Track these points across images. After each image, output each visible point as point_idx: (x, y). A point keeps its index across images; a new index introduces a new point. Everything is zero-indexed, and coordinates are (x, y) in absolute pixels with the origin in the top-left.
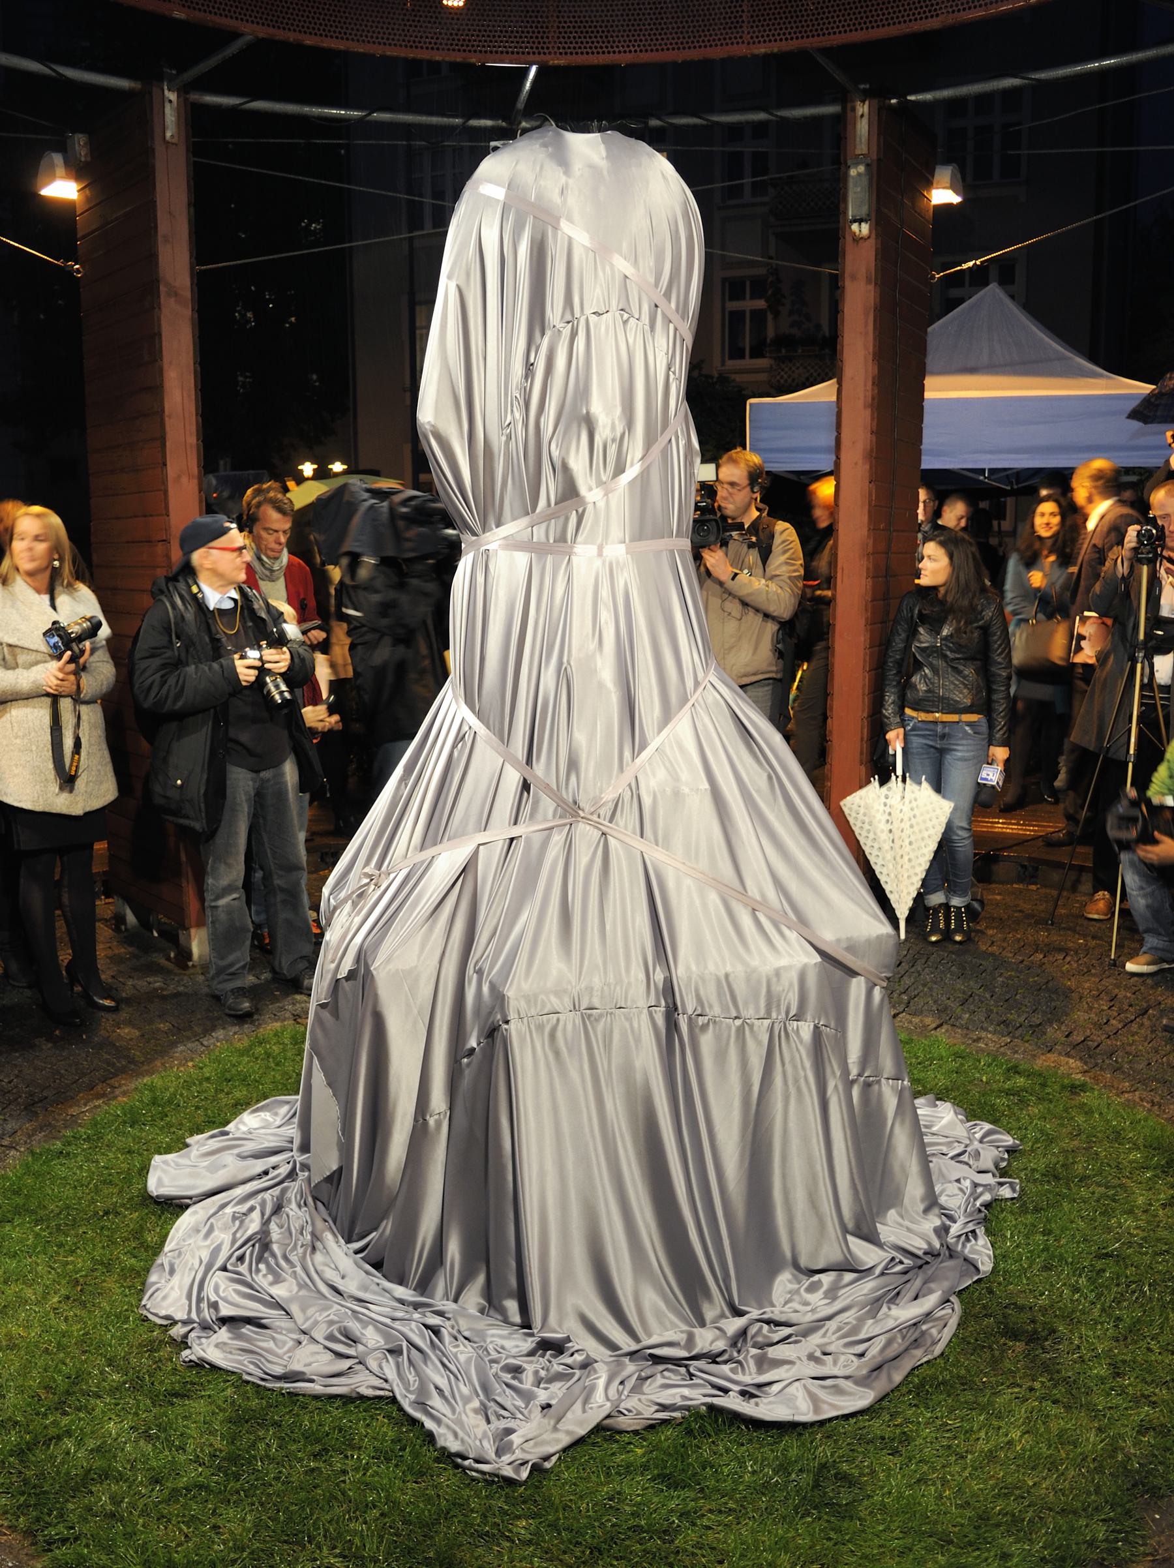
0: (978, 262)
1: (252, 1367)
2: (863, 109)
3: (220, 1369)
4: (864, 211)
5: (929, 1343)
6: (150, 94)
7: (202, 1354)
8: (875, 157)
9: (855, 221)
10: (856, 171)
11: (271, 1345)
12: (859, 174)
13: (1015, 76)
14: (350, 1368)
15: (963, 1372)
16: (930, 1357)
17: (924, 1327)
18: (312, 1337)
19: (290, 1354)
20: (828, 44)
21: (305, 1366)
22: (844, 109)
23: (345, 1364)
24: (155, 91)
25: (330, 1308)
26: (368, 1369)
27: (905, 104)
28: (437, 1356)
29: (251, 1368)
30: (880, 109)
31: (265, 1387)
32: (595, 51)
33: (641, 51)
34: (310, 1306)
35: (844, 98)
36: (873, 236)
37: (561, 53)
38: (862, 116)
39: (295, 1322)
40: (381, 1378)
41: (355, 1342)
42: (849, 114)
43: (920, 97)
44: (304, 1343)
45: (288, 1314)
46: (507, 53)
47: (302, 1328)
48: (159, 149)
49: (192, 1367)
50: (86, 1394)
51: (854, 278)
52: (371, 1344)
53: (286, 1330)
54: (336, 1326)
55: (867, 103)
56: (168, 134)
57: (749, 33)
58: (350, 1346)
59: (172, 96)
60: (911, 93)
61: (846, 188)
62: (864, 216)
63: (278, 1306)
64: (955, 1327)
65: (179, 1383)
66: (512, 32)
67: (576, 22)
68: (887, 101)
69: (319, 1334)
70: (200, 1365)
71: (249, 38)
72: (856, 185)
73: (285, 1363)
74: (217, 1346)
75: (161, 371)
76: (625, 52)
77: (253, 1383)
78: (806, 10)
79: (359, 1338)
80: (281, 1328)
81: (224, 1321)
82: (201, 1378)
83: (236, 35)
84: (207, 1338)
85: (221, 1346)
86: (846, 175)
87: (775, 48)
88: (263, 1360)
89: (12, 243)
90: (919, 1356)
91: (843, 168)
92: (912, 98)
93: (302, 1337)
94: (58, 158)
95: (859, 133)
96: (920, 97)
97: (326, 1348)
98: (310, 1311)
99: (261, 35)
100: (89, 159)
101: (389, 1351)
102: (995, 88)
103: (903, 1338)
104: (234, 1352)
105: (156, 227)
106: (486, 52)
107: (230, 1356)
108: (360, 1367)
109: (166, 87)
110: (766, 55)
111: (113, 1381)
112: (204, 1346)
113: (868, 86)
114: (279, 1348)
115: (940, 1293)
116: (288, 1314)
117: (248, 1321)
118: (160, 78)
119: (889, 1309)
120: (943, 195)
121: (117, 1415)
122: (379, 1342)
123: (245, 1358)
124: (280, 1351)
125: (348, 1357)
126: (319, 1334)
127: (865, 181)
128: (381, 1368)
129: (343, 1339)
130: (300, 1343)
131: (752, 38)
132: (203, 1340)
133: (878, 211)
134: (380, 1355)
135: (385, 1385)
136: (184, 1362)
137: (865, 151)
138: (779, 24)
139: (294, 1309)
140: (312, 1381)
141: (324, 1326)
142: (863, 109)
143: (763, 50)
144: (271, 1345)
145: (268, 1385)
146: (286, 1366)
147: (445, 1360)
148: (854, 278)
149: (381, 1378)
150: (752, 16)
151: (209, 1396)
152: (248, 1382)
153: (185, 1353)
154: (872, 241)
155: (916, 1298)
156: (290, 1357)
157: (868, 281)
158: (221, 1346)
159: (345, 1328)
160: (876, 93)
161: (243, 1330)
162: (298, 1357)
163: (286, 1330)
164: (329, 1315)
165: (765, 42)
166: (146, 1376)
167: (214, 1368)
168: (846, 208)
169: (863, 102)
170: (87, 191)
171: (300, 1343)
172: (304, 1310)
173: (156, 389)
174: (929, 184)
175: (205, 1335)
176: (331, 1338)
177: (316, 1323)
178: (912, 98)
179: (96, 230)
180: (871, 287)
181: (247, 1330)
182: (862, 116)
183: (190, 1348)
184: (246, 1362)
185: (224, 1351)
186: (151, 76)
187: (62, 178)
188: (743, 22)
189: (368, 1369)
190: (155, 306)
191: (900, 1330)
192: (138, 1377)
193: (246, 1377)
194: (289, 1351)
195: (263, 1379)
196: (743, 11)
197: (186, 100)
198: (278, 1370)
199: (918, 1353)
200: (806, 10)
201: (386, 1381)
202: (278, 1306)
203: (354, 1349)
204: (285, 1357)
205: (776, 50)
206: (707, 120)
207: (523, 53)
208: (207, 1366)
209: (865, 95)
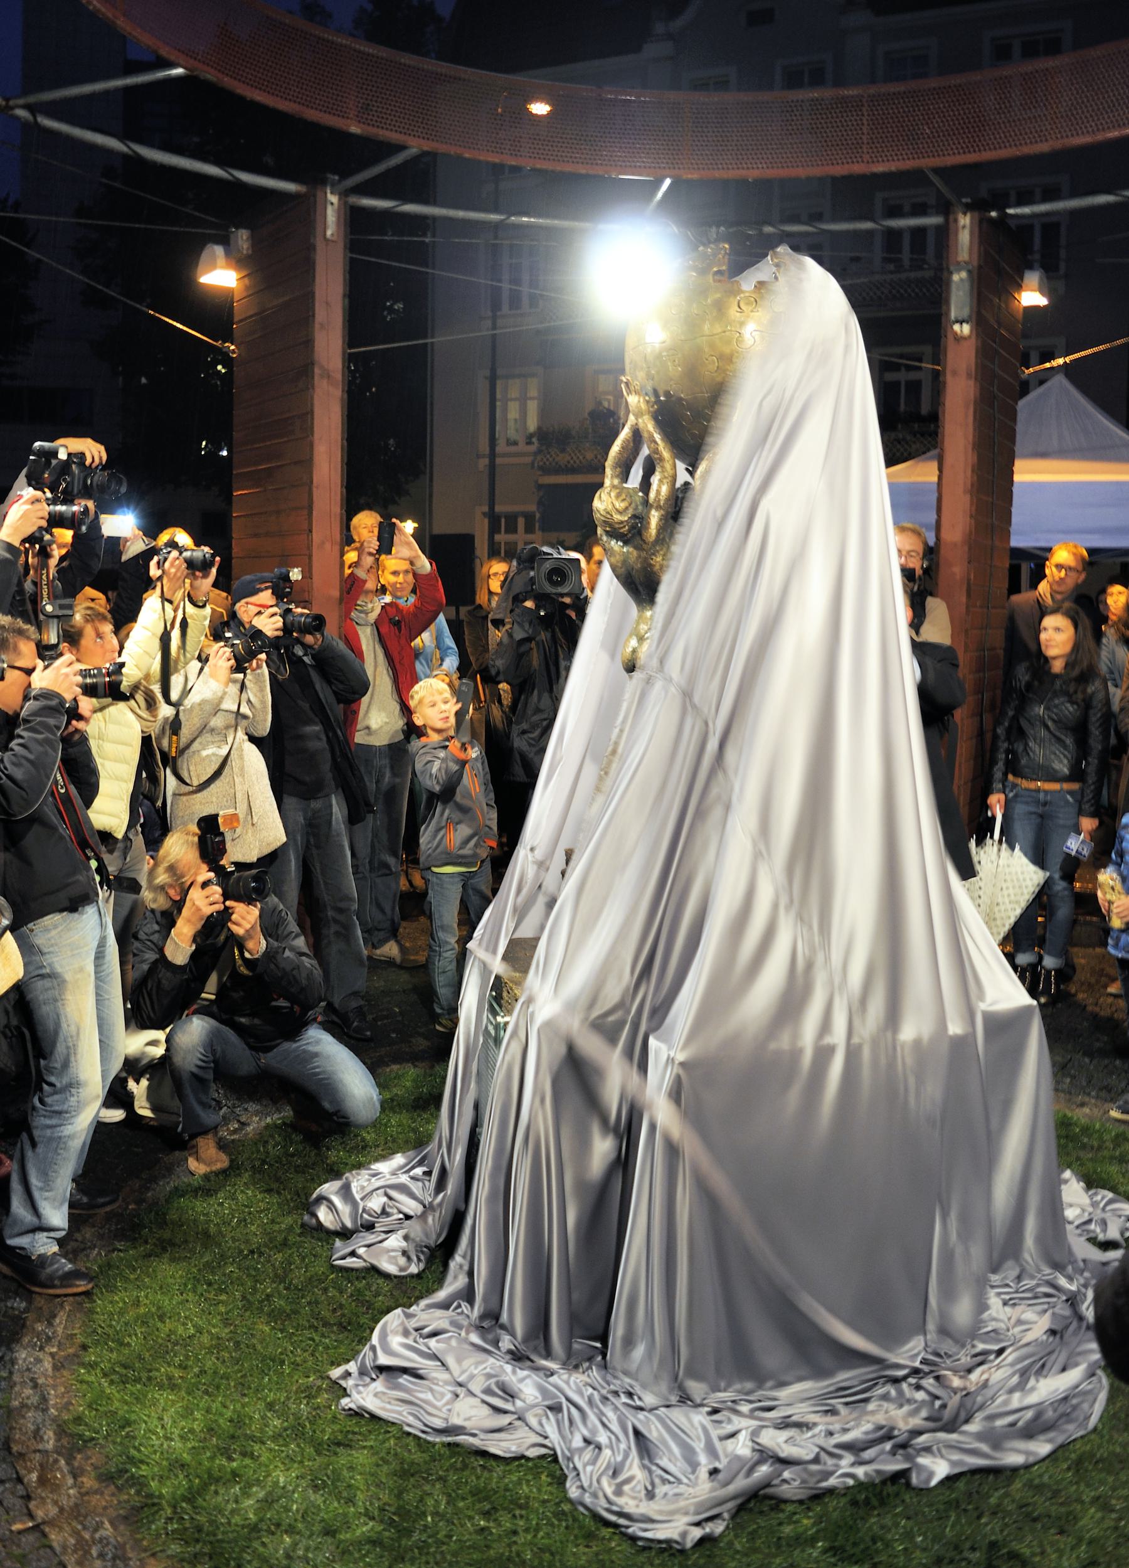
2: (965, 220)
4: (966, 312)
5: (1082, 1418)
6: (315, 196)
7: (362, 1403)
8: (975, 263)
9: (957, 321)
10: (959, 277)
11: (428, 1396)
12: (961, 280)
13: (1109, 192)
15: (1118, 1450)
17: (1074, 1401)
19: (449, 1407)
21: (466, 1420)
23: (504, 1420)
24: (319, 194)
25: (486, 1361)
26: (527, 1425)
27: (1004, 216)
28: (595, 1414)
29: (411, 1420)
30: (981, 222)
31: (426, 1441)
34: (466, 1358)
35: (946, 209)
36: (974, 337)
38: (964, 227)
39: (451, 1373)
40: (541, 1435)
41: (512, 1397)
42: (952, 225)
44: (461, 1396)
45: (443, 1365)
47: (460, 1380)
48: (320, 245)
49: (351, 1415)
50: (252, 1438)
51: (955, 373)
52: (530, 1400)
54: (493, 1380)
56: (329, 233)
58: (507, 1400)
59: (334, 199)
60: (1010, 207)
63: (435, 1357)
65: (341, 1432)
69: (476, 1387)
70: (357, 1414)
71: (414, 151)
73: (445, 1416)
74: (376, 1395)
77: (415, 1436)
81: (382, 1369)
82: (361, 1427)
83: (402, 148)
84: (364, 1386)
86: (948, 282)
89: (175, 323)
90: (1073, 1431)
91: (945, 274)
92: (1011, 211)
93: (459, 1390)
94: (219, 250)
97: (484, 1402)
98: (466, 1363)
99: (425, 148)
100: (250, 252)
101: (550, 1408)
104: (393, 1402)
105: (314, 316)
107: (388, 1406)
108: (518, 1423)
109: (329, 191)
111: (275, 1427)
113: (969, 200)
114: (439, 1401)
116: (443, 1365)
117: (405, 1371)
118: (324, 182)
120: (1032, 297)
123: (404, 1409)
124: (439, 1404)
125: (505, 1412)
126: (476, 1387)
127: (967, 286)
128: (541, 1424)
129: (500, 1393)
130: (457, 1396)
132: (361, 1388)
135: (546, 1442)
136: (344, 1410)
139: (450, 1361)
140: (474, 1435)
141: (482, 1379)
142: (965, 220)
145: (429, 1438)
146: (446, 1420)
147: (604, 1419)
151: (372, 1447)
152: (409, 1434)
153: (345, 1402)
155: (1064, 1370)
156: (450, 1410)
157: (969, 376)
159: (503, 1383)
160: (978, 206)
161: (401, 1380)
167: (374, 1417)
168: (949, 310)
169: (965, 214)
170: (246, 281)
172: (459, 1361)
174: (1019, 287)
175: (361, 1383)
176: (488, 1391)
178: (1011, 211)
179: (251, 316)
180: (971, 383)
181: (404, 1380)
182: (964, 227)
183: (349, 1396)
184: (405, 1413)
185: (383, 1401)
186: (315, 178)
187: (222, 267)
189: (527, 1425)
193: (407, 1429)
194: (447, 1403)
195: (423, 1432)
197: (346, 203)
198: (439, 1423)
199: (1071, 1427)
201: (546, 1438)
202: (435, 1357)
205: (893, 169)
208: (367, 1415)
209: (968, 208)
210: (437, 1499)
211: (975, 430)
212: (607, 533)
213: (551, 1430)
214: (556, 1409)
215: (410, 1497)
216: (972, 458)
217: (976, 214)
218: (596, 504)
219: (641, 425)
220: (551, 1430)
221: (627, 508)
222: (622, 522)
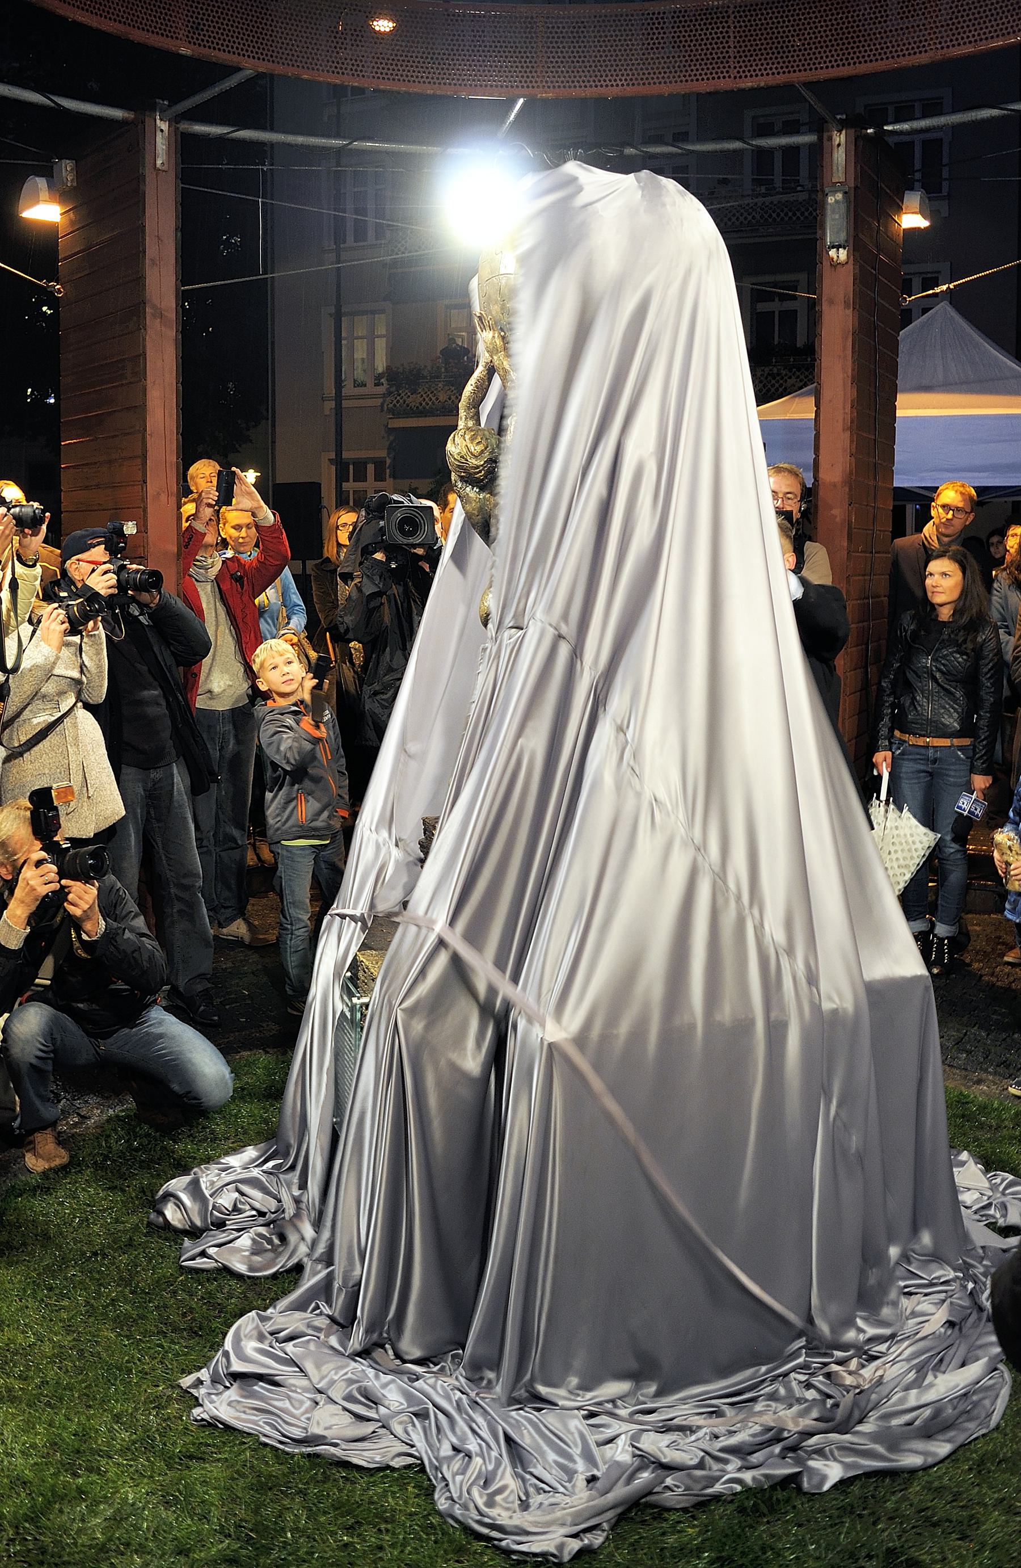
0: (951, 286)
1: (268, 1428)
2: (840, 138)
3: (235, 1429)
4: (843, 236)
9: (833, 247)
11: (286, 1404)
12: (837, 201)
14: (374, 1432)
16: (984, 1431)
18: (329, 1397)
20: (814, 79)
21: (326, 1429)
22: (820, 139)
23: (368, 1428)
25: (347, 1366)
26: (392, 1434)
27: (881, 134)
29: (267, 1430)
31: (283, 1451)
32: (583, 85)
33: (628, 85)
35: (820, 127)
36: (851, 262)
37: (549, 87)
38: (839, 145)
39: (309, 1379)
40: (407, 1444)
41: (376, 1404)
42: (826, 143)
43: (897, 127)
44: (321, 1403)
45: (302, 1371)
46: (496, 86)
50: (98, 1452)
51: (831, 302)
52: (394, 1406)
53: (300, 1388)
55: (844, 132)
57: (735, 67)
58: (371, 1408)
60: (888, 124)
61: (823, 215)
62: (842, 243)
64: (1007, 1399)
65: (194, 1444)
66: (501, 67)
67: (564, 57)
68: (864, 131)
69: (337, 1394)
70: (211, 1425)
72: (833, 212)
74: (229, 1404)
75: (145, 390)
76: (612, 85)
77: (272, 1446)
78: (793, 46)
79: (380, 1399)
80: (294, 1386)
81: (236, 1376)
85: (234, 1404)
86: (824, 203)
87: (762, 82)
88: (279, 1421)
91: (820, 195)
93: (318, 1397)
95: (835, 161)
96: (897, 127)
98: (325, 1369)
101: (415, 1415)
102: (974, 118)
103: (955, 1408)
104: (248, 1411)
106: (486, 86)
107: (243, 1416)
110: (752, 89)
111: (123, 1440)
112: (217, 1405)
113: (844, 117)
115: (986, 1359)
116: (302, 1371)
117: (260, 1377)
119: (936, 1377)
120: (912, 220)
121: (132, 1479)
122: (402, 1404)
123: (261, 1419)
126: (337, 1394)
127: (843, 208)
129: (363, 1400)
130: (317, 1403)
131: (738, 72)
133: (856, 236)
134: (406, 1418)
135: (412, 1451)
136: (196, 1420)
137: (842, 180)
138: (766, 59)
139: (309, 1366)
140: (335, 1445)
141: (343, 1384)
142: (840, 138)
143: (750, 84)
144: (286, 1404)
146: (305, 1429)
148: (831, 302)
149: (407, 1444)
150: (739, 52)
152: (266, 1445)
153: (196, 1411)
154: (850, 266)
156: (308, 1419)
157: (847, 305)
158: (234, 1404)
159: (365, 1388)
160: (852, 123)
161: (256, 1388)
162: (317, 1418)
163: (300, 1388)
164: (346, 1374)
165: (751, 76)
166: (157, 1436)
167: (228, 1428)
168: (824, 234)
169: (840, 131)
171: (317, 1403)
172: (318, 1367)
173: (140, 409)
174: (899, 209)
175: (215, 1391)
176: (349, 1398)
177: (332, 1383)
181: (260, 1387)
183: (201, 1405)
184: (261, 1423)
188: (729, 57)
190: (141, 326)
191: (951, 1400)
192: (148, 1436)
194: (306, 1412)
195: (281, 1442)
196: (729, 47)
198: (297, 1433)
200: (793, 46)
201: (412, 1446)
203: (374, 1411)
204: (303, 1419)
205: (762, 84)
206: (682, 149)
207: (512, 87)
208: (221, 1426)
209: (842, 125)
210: (297, 1514)
211: (853, 362)
212: (462, 478)
213: (417, 1438)
214: (422, 1415)
215: (267, 1512)
216: (851, 393)
217: (852, 131)
218: (450, 447)
219: (496, 363)
220: (417, 1438)
221: (482, 452)
222: (478, 467)
